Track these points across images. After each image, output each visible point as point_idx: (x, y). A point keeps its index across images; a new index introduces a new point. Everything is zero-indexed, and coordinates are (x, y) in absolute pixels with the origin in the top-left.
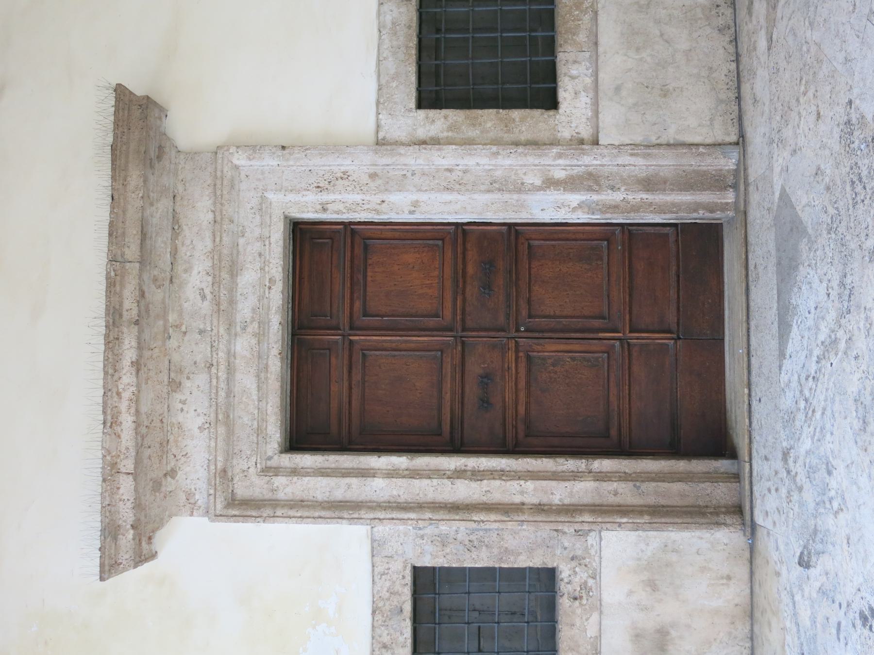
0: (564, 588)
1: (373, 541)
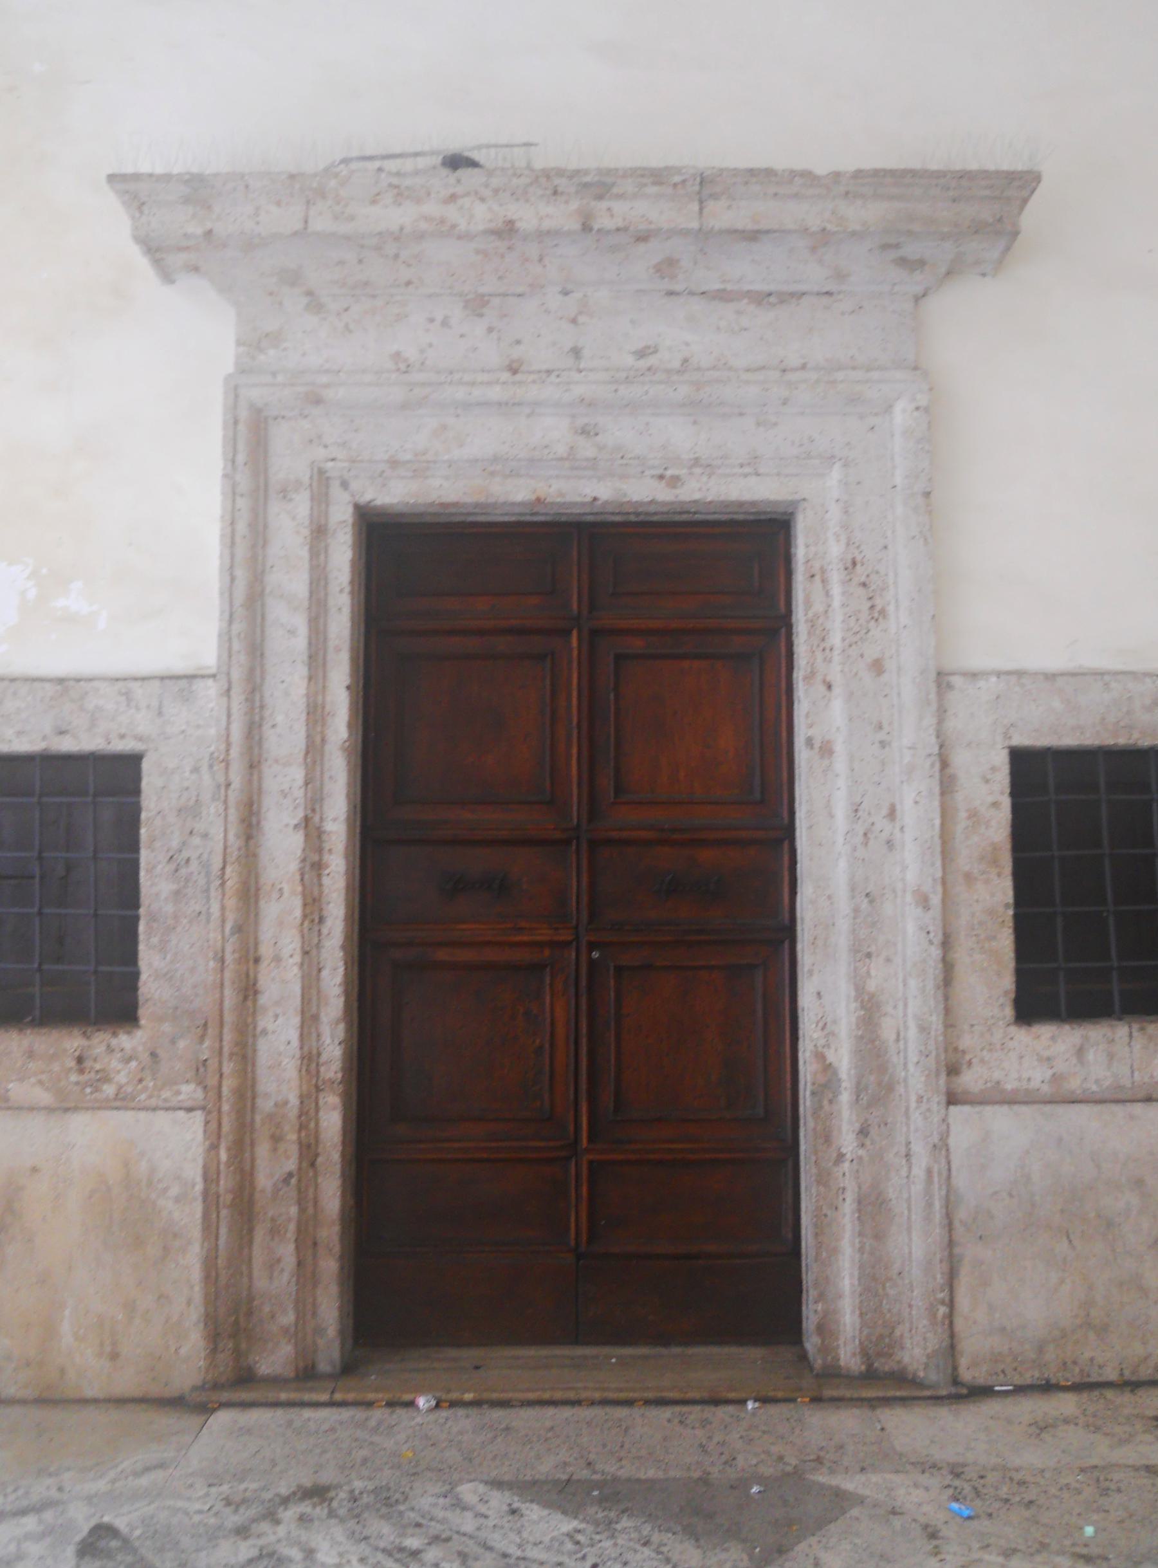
1: (191, 677)
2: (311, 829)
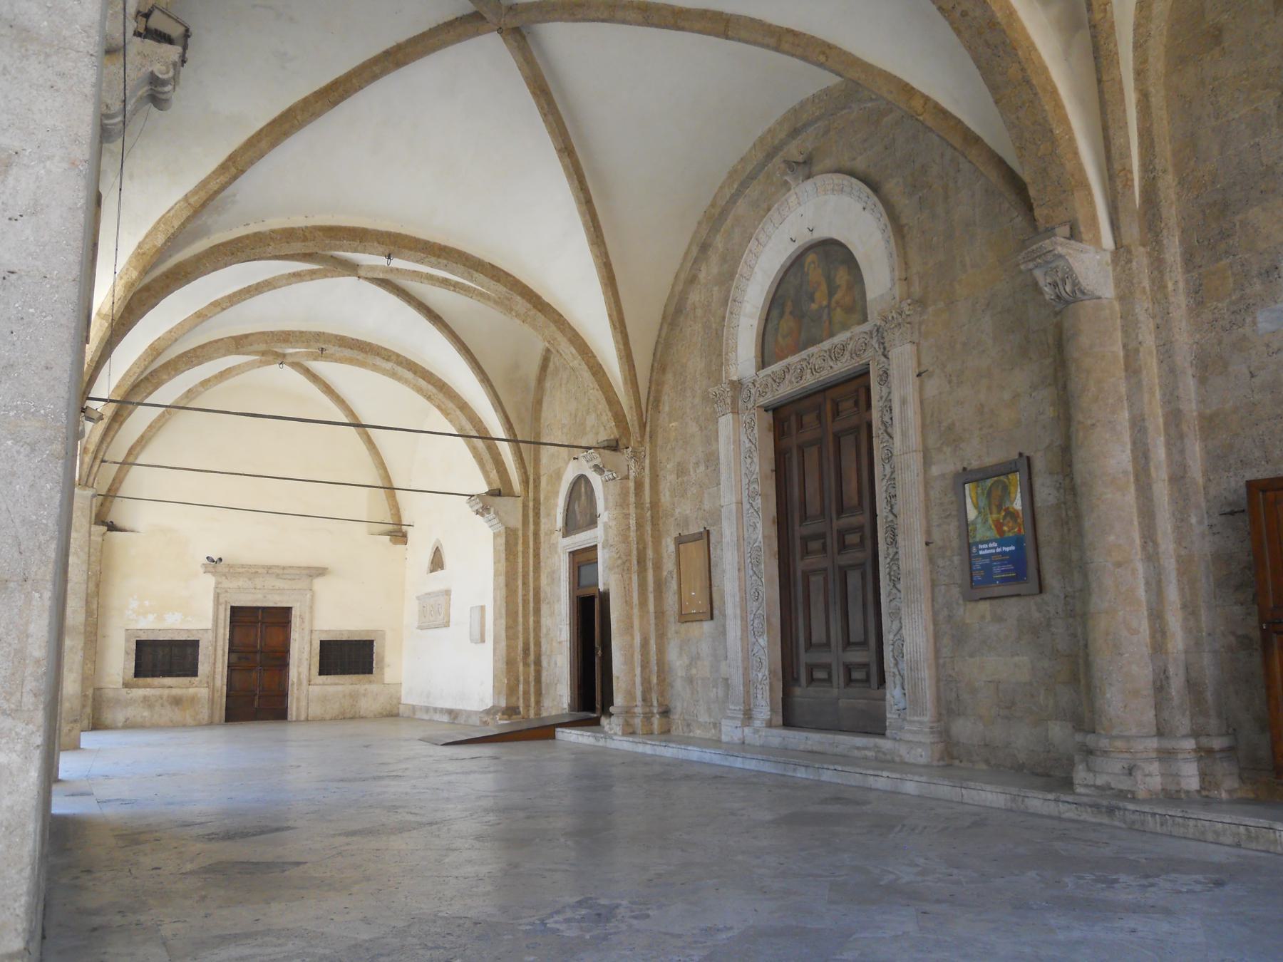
0: (193, 679)
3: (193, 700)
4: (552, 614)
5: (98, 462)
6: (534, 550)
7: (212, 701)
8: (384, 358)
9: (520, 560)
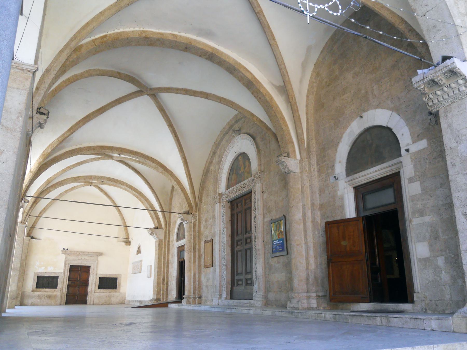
2: (66, 280)
3: (55, 297)
4: (172, 268)
5: (28, 216)
6: (168, 247)
7: (61, 297)
8: (122, 184)
9: (163, 250)
